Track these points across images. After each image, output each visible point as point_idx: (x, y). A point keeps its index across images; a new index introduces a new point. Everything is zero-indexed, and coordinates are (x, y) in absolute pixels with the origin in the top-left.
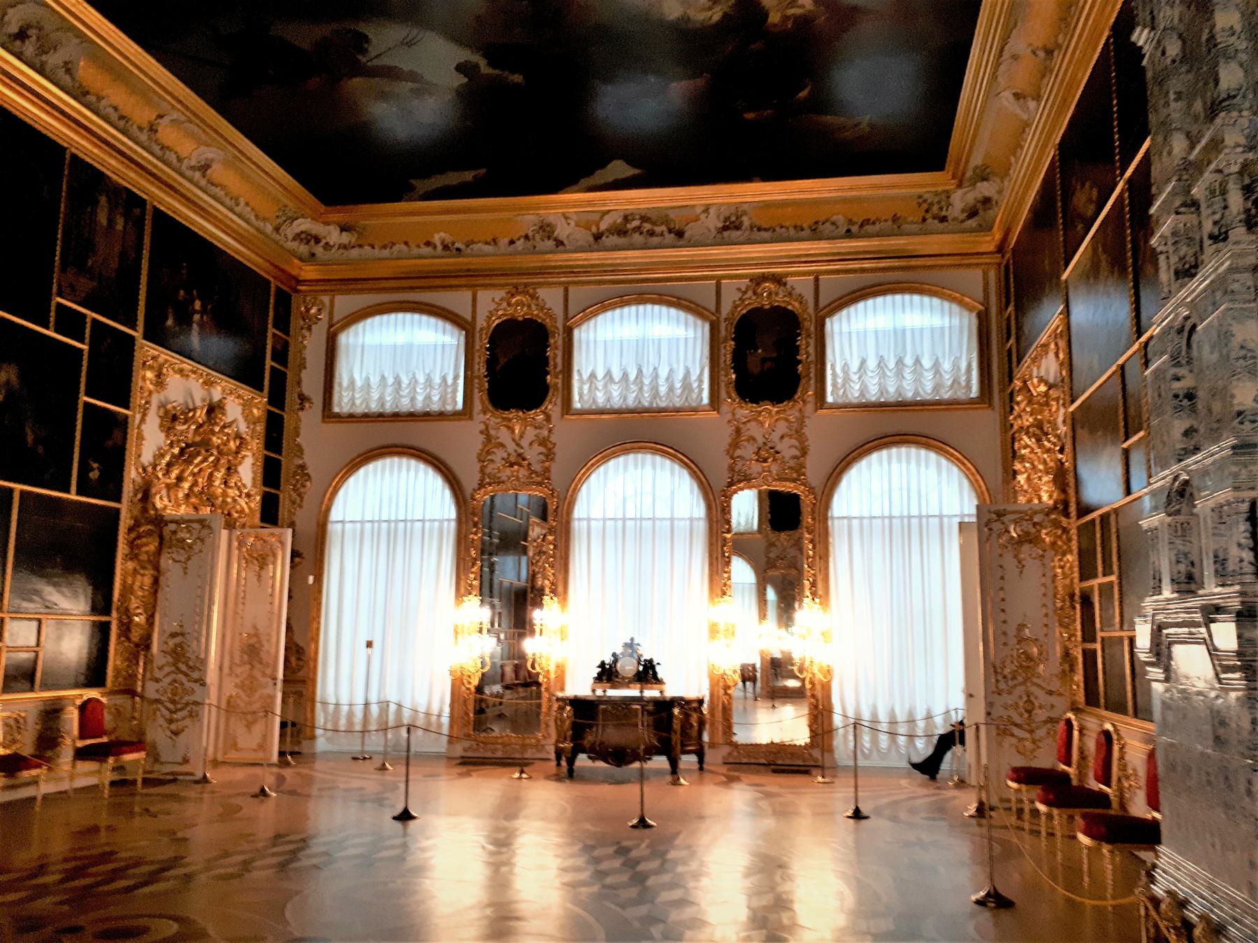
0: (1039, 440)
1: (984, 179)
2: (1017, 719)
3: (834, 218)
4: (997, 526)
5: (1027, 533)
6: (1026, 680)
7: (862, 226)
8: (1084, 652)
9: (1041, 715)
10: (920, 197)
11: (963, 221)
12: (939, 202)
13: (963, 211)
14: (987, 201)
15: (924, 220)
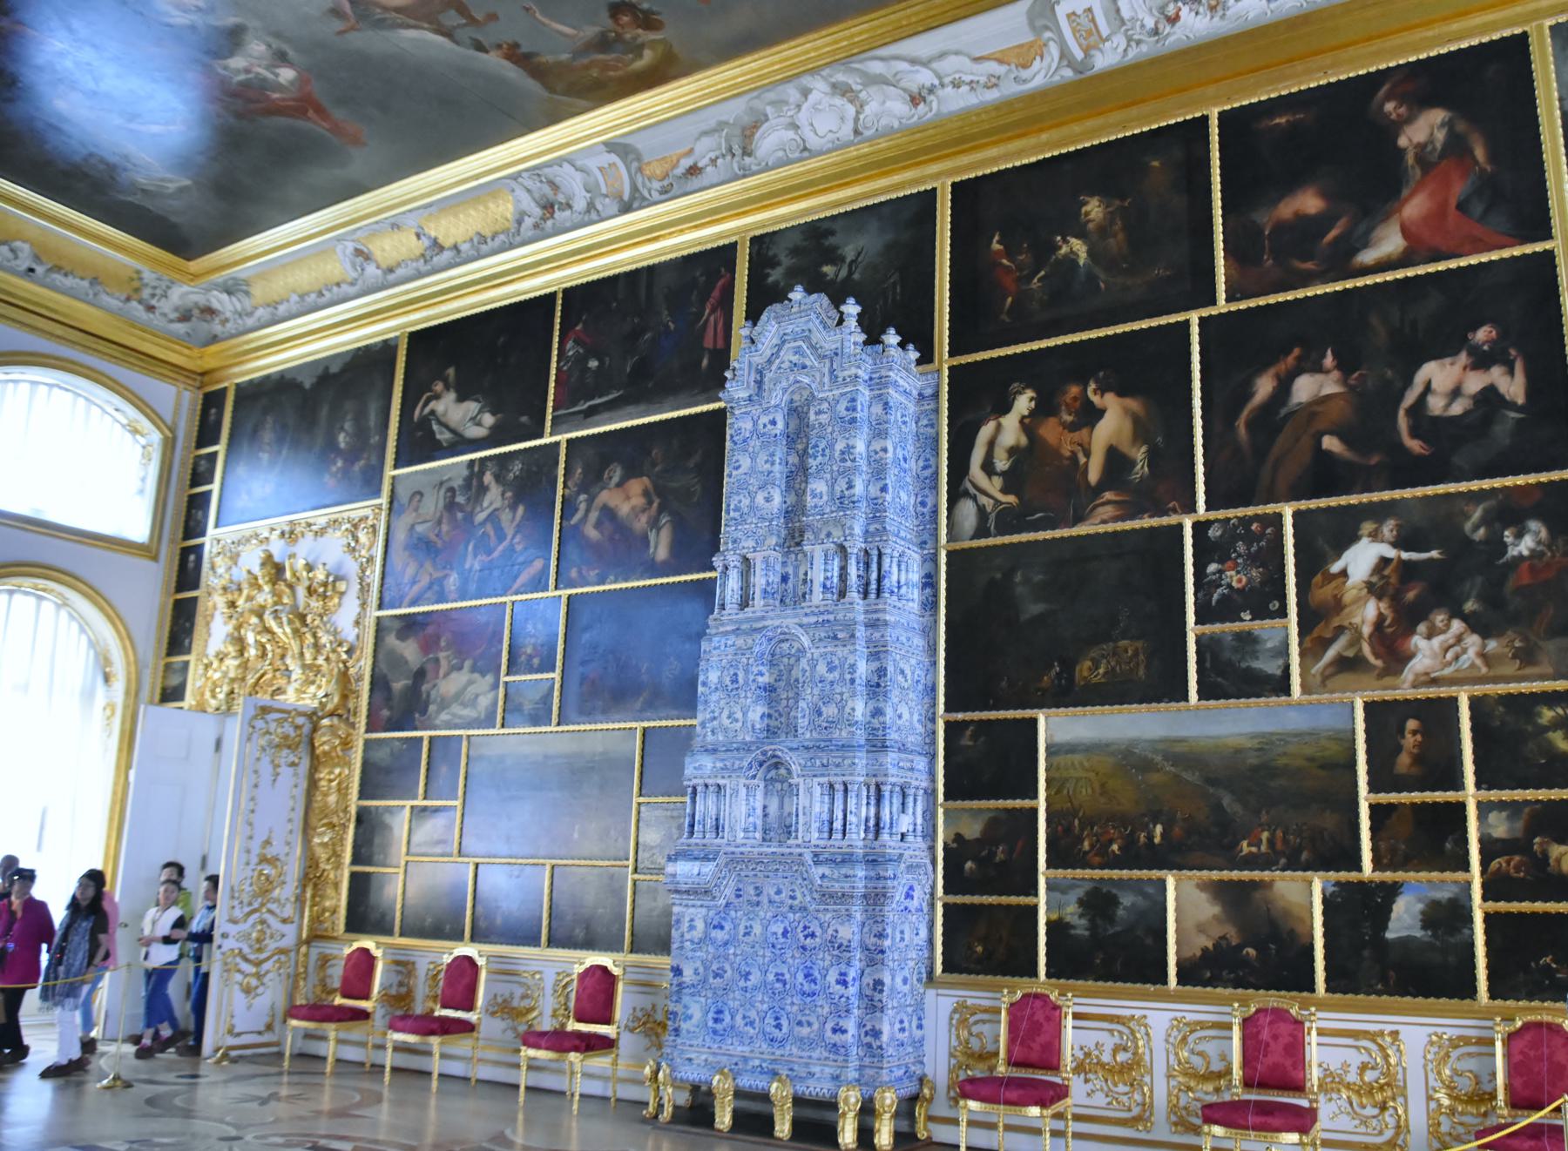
0: (296, 632)
1: (229, 293)
2: (246, 950)
3: (18, 244)
4: (260, 724)
5: (286, 737)
6: (263, 905)
7: (50, 270)
8: (354, 877)
9: (272, 945)
10: (138, 272)
11: (171, 321)
12: (155, 288)
13: (176, 309)
14: (209, 312)
15: (128, 299)
